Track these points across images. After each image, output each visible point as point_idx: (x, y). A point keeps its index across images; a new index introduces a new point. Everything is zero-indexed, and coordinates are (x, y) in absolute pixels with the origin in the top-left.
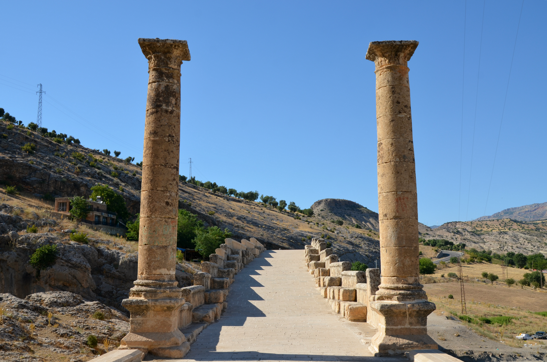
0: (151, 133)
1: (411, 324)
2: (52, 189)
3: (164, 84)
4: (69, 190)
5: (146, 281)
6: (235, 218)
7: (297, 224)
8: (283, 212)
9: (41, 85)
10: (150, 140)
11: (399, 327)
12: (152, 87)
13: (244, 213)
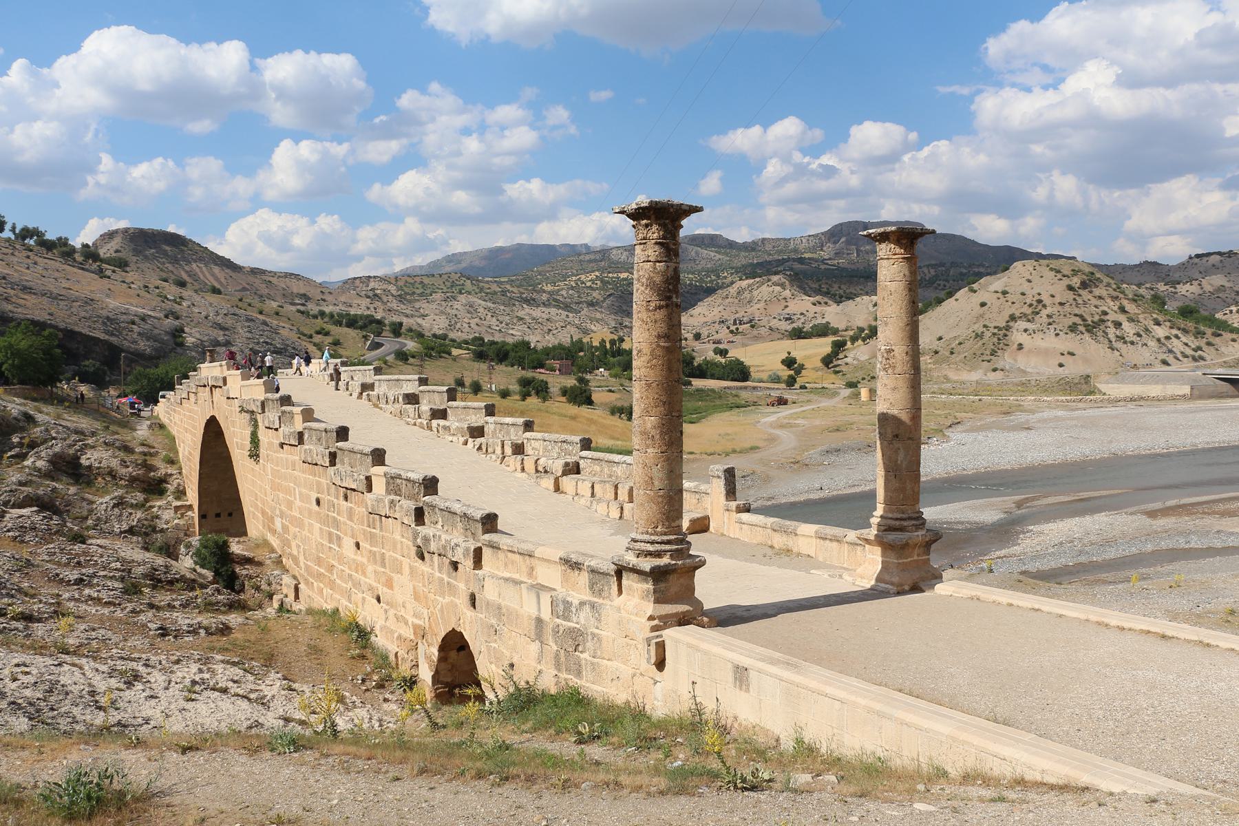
0: (659, 337)
1: (918, 555)
3: (672, 265)
5: (665, 538)
7: (109, 289)
10: (658, 346)
11: (909, 559)
12: (655, 268)
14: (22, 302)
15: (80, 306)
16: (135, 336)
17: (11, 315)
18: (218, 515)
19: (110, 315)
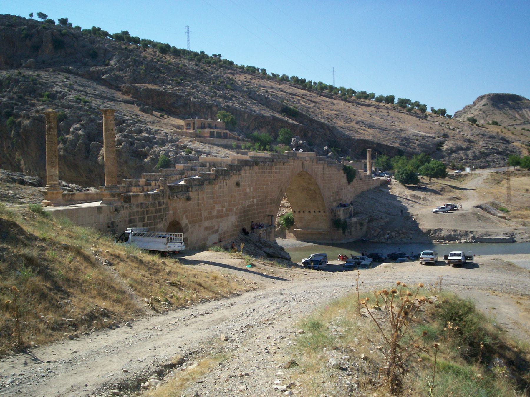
2: (193, 110)
4: (205, 110)
6: (353, 124)
8: (412, 113)
9: (188, 27)
13: (365, 118)
14: (362, 131)
15: (393, 133)
16: (416, 145)
17: (353, 137)
18: (299, 212)
19: (407, 137)
